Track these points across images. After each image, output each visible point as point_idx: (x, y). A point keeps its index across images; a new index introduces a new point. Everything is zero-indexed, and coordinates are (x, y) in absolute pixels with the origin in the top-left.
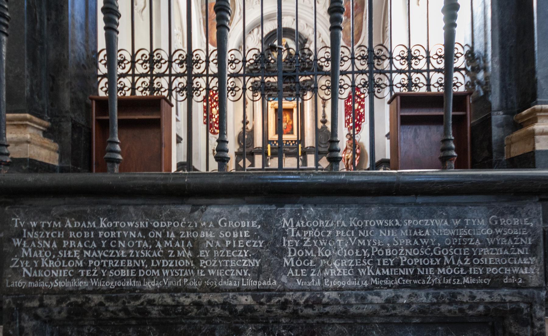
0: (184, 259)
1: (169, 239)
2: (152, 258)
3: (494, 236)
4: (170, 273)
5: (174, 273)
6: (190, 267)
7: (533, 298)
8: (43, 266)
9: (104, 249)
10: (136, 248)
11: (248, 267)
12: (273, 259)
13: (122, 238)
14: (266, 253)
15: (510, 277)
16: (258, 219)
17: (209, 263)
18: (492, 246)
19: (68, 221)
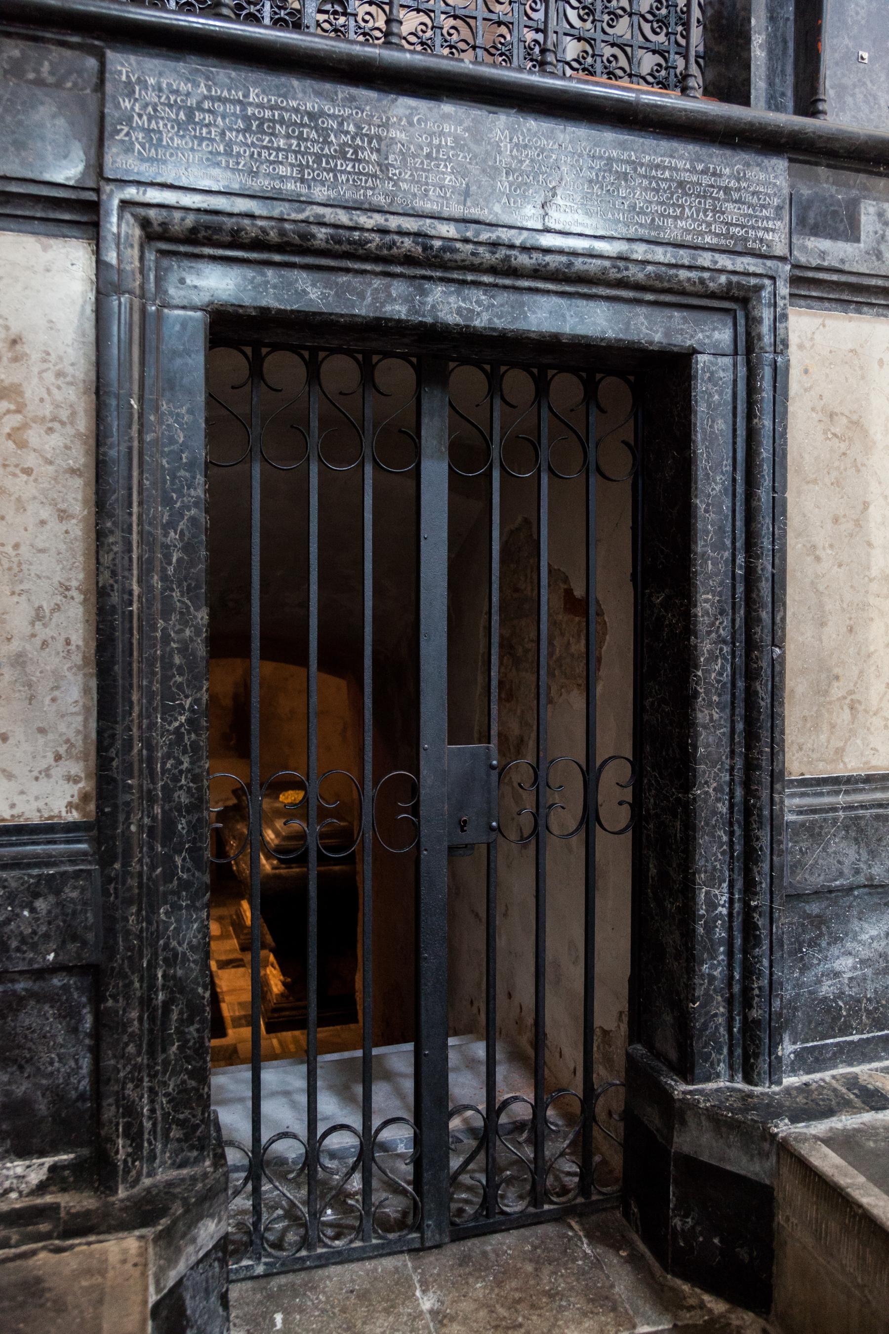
0: (368, 162)
1: (347, 133)
2: (324, 156)
3: (739, 190)
4: (348, 180)
5: (354, 180)
6: (375, 176)
7: (777, 271)
8: (164, 143)
9: (255, 133)
10: (300, 137)
11: (453, 187)
12: (484, 179)
13: (282, 122)
14: (475, 169)
15: (754, 241)
16: (466, 125)
17: (400, 174)
18: (736, 202)
19: (202, 85)
